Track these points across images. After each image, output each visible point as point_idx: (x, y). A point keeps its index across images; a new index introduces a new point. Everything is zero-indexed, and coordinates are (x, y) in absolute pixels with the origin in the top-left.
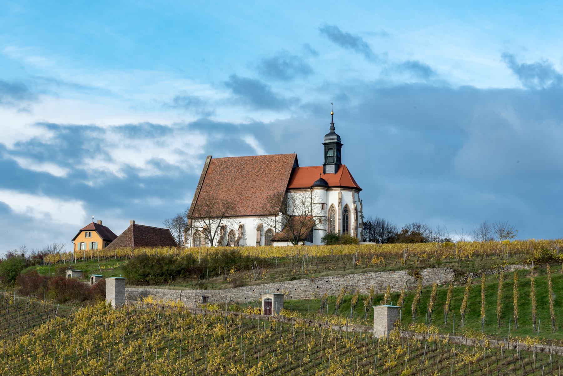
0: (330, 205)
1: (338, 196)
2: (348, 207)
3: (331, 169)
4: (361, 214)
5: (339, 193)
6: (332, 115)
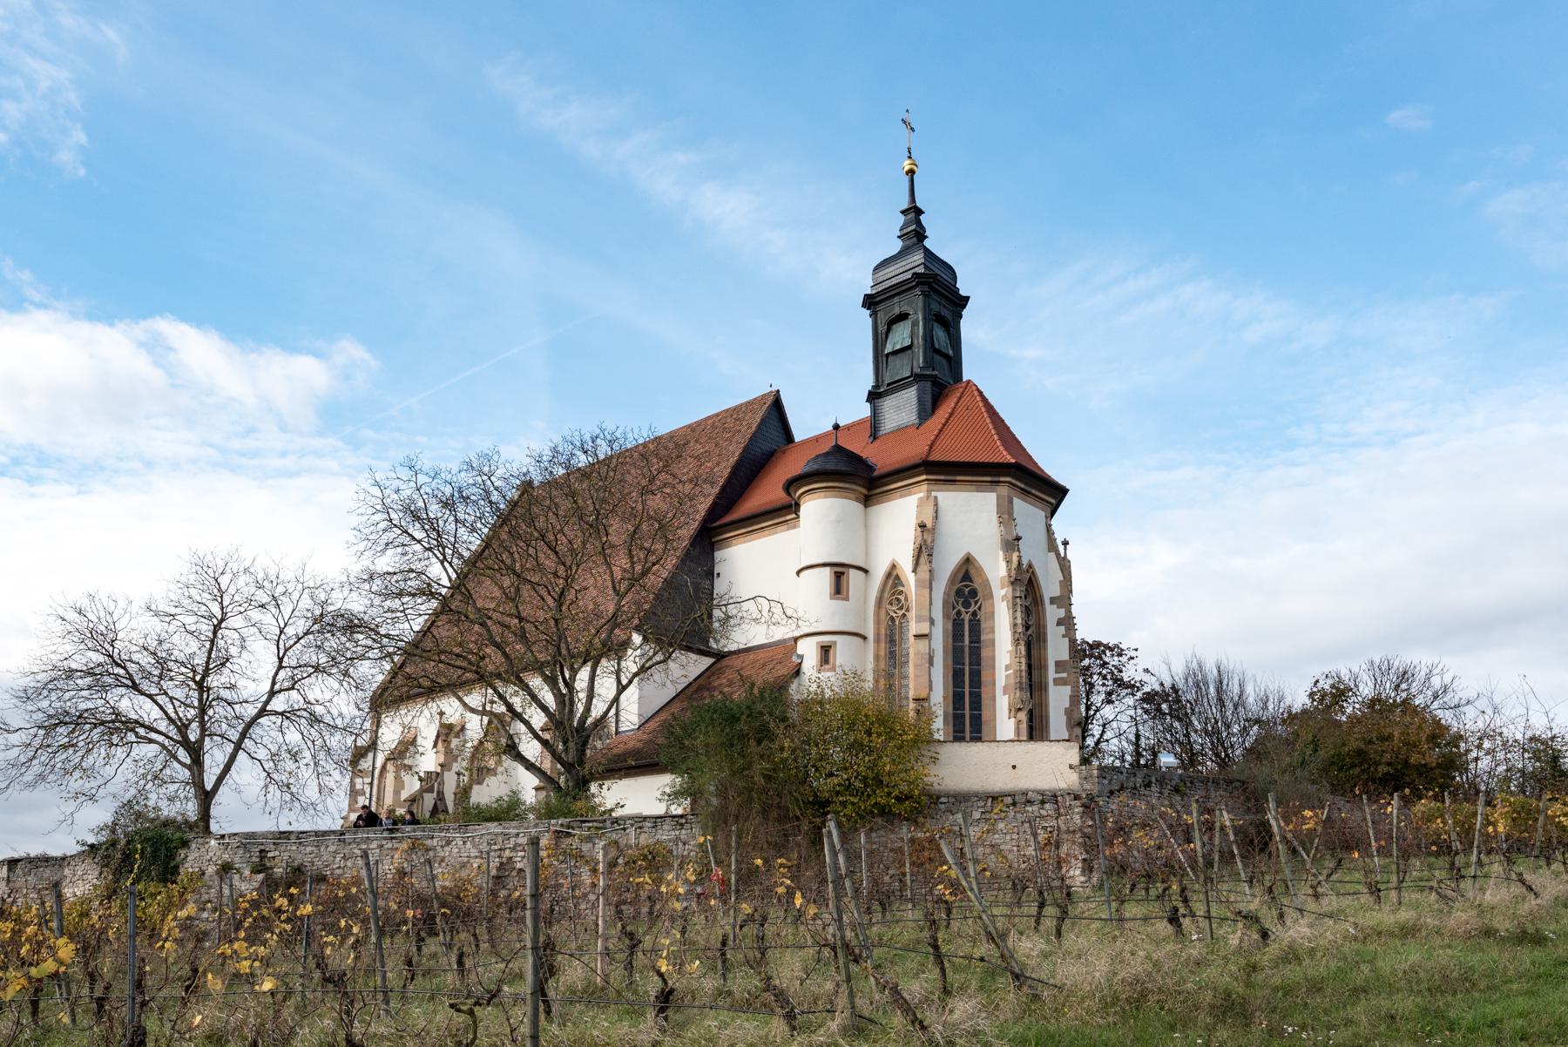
0: (879, 572)
1: (919, 513)
2: (980, 570)
3: (901, 409)
4: (1062, 613)
5: (921, 504)
6: (911, 172)
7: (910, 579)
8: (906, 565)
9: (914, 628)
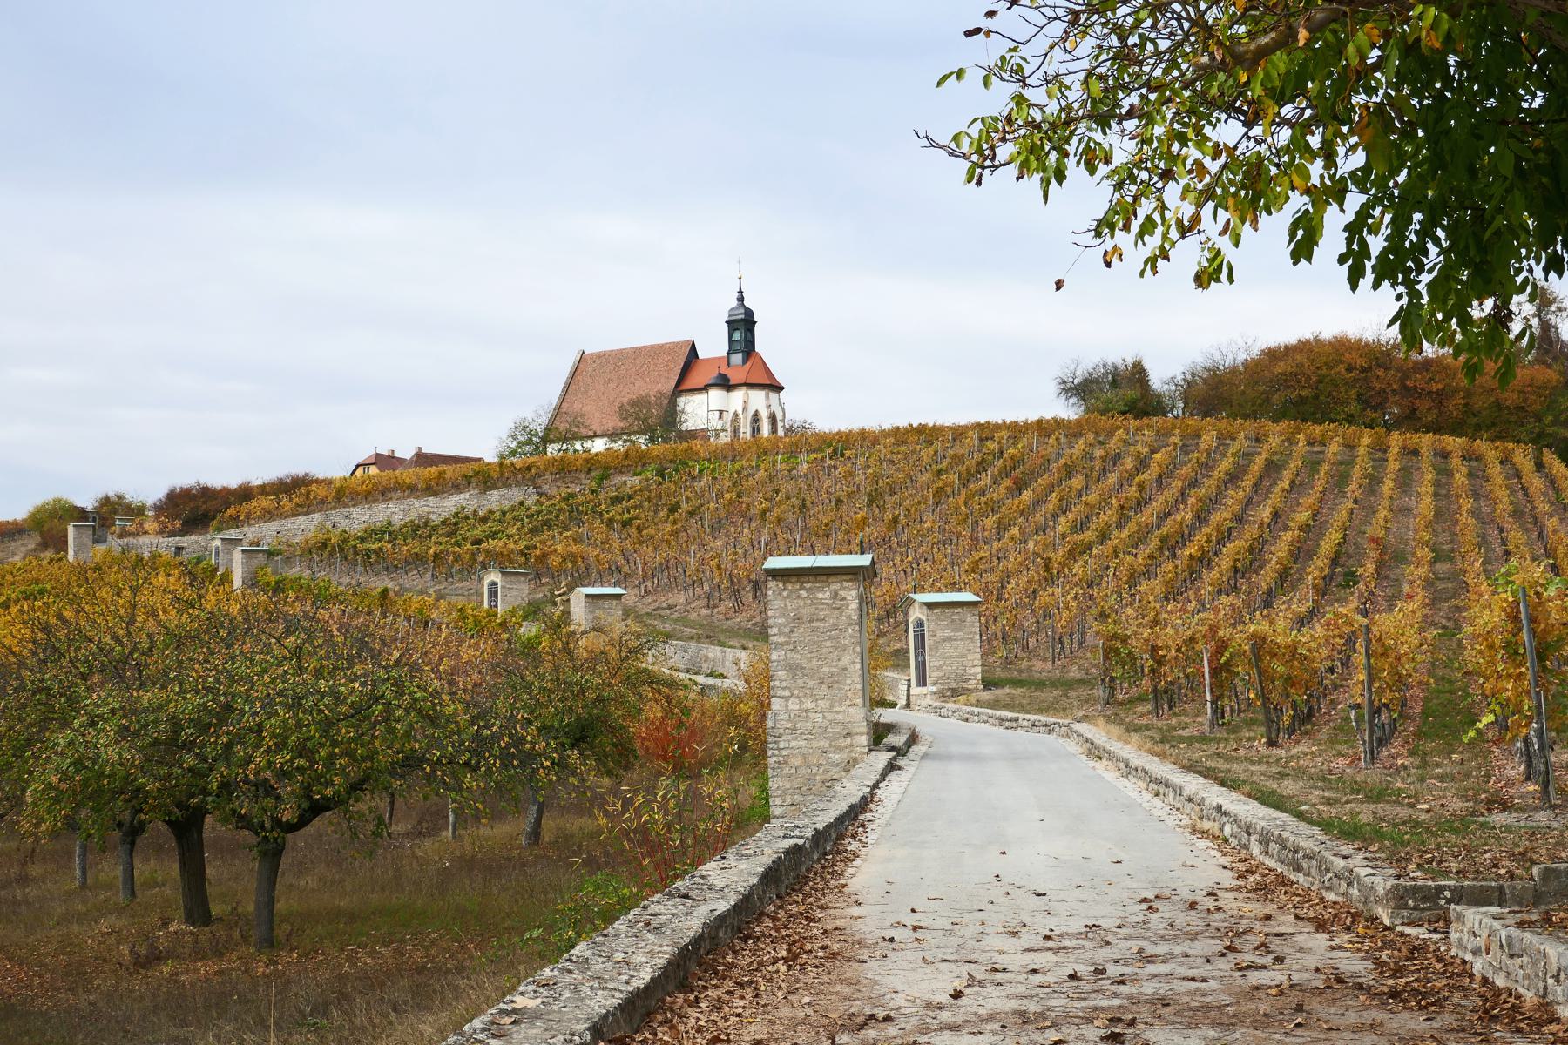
3: (737, 358)
7: (741, 416)
8: (740, 412)
9: (742, 430)
